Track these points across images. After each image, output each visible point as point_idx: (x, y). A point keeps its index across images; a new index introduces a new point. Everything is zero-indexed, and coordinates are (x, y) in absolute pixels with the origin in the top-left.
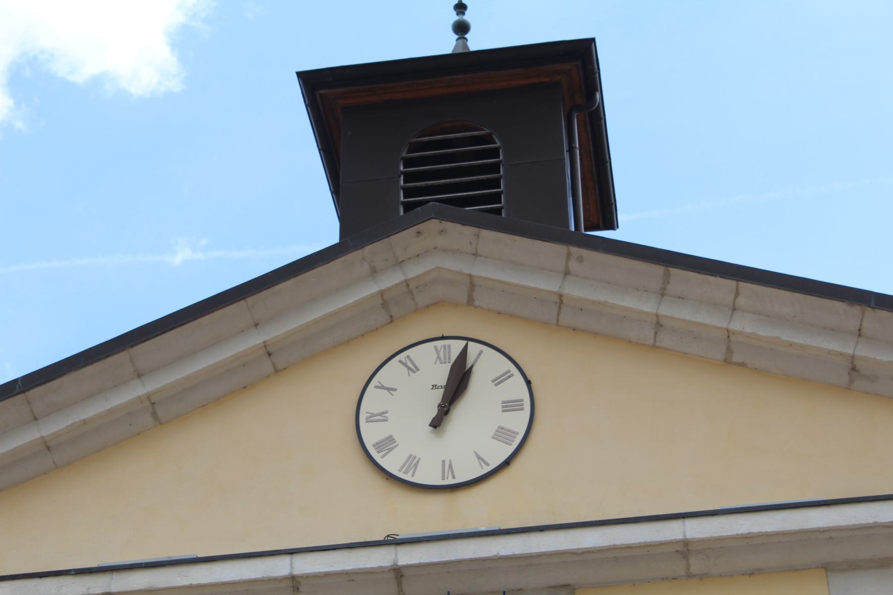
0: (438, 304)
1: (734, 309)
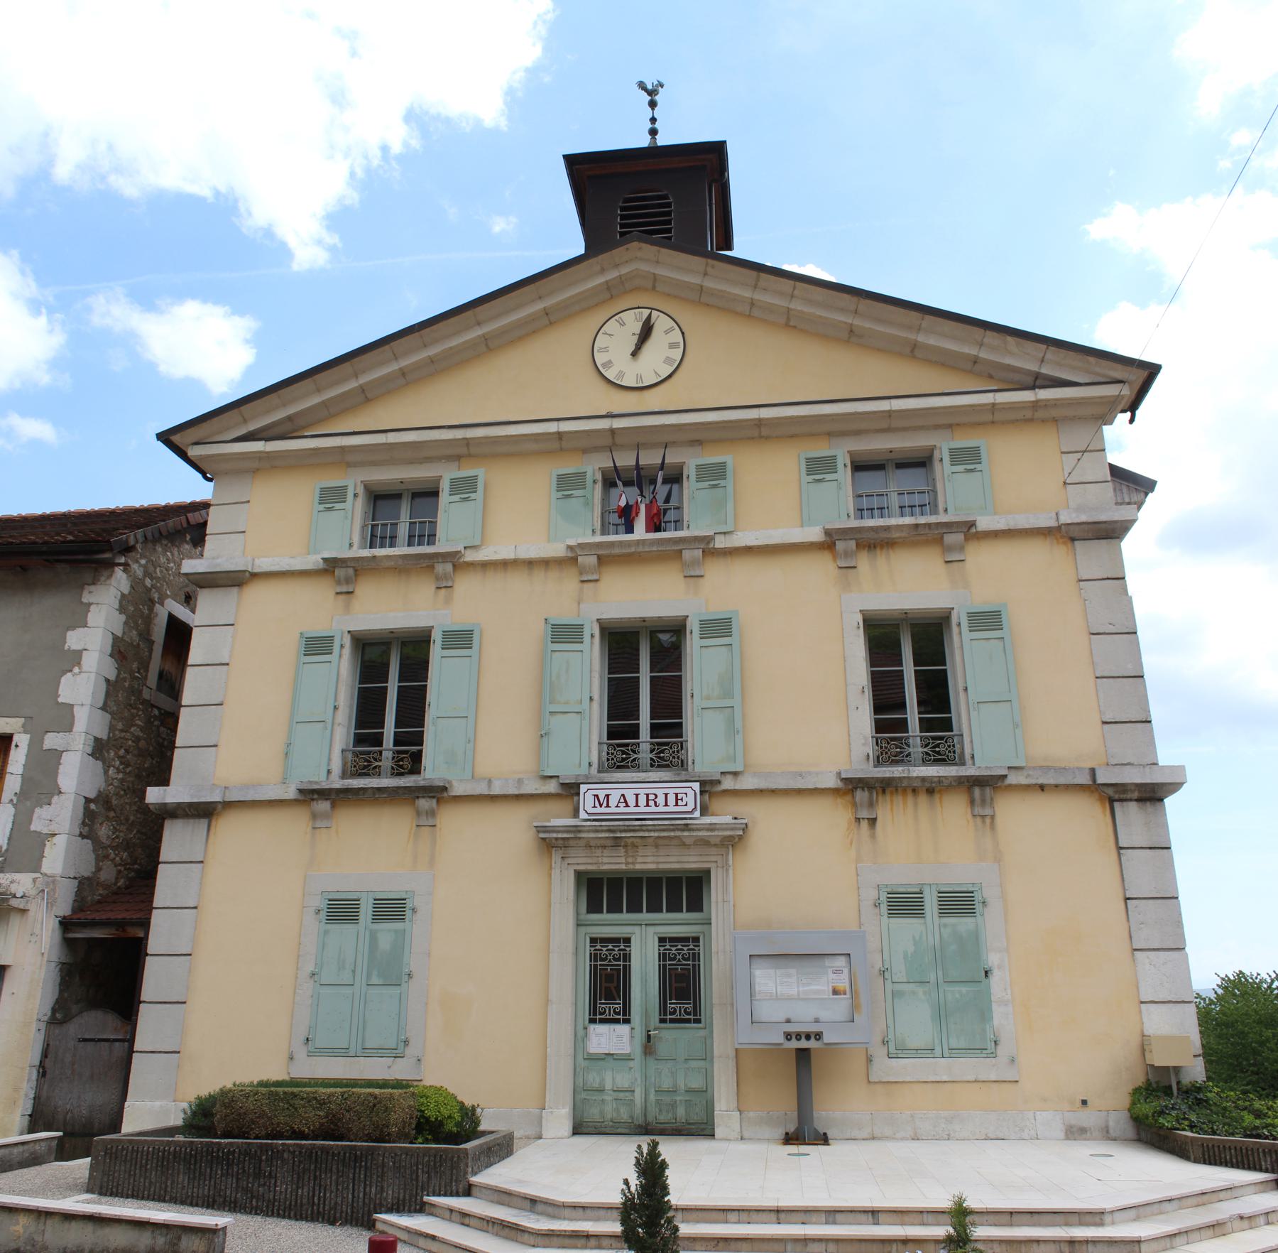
0: (637, 289)
1: (792, 296)
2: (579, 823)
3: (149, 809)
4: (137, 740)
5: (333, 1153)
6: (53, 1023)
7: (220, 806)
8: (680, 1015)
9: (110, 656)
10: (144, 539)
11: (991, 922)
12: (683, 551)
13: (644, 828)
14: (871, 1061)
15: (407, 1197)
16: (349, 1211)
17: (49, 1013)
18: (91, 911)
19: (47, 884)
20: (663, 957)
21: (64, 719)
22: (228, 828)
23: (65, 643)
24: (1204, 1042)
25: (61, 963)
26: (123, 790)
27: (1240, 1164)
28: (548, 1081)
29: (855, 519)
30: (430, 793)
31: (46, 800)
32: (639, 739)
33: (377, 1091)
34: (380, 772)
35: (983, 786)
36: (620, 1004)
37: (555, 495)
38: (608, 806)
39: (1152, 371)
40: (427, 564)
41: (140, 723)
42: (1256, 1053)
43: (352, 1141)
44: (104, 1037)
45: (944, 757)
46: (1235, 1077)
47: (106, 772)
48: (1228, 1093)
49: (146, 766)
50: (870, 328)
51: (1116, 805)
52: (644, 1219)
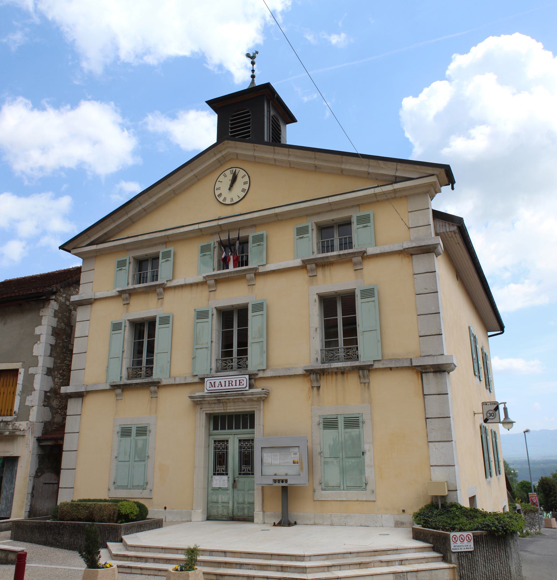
11: (366, 430)
17: (35, 474)
51: (424, 375)
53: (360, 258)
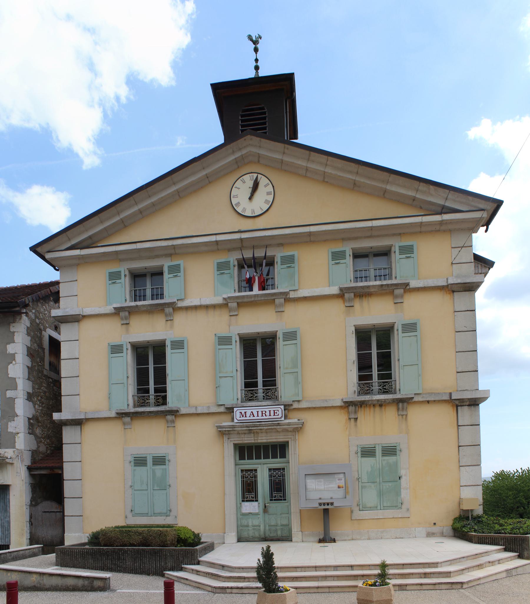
0: (250, 162)
1: (326, 165)
2: (234, 424)
3: (55, 421)
4: (45, 392)
5: (146, 551)
6: (32, 506)
7: (84, 420)
8: (278, 498)
9: (27, 355)
10: (32, 300)
11: (402, 458)
12: (276, 300)
13: (261, 425)
14: (352, 512)
15: (176, 566)
16: (154, 571)
17: (30, 502)
18: (38, 463)
19: (19, 453)
20: (270, 476)
21: (13, 384)
22: (89, 429)
23: (7, 350)
24: (485, 497)
25: (30, 483)
26: (43, 414)
27: (491, 543)
28: (226, 524)
29: (354, 282)
30: (172, 413)
31: (12, 419)
32: (258, 387)
33: (161, 529)
34: (150, 405)
35: (403, 402)
36: (254, 494)
37: (217, 273)
38: (246, 417)
39: (499, 204)
40: (160, 309)
41: (45, 385)
42: (504, 500)
43: (153, 547)
44: (52, 511)
45: (387, 390)
46: (495, 510)
47: (34, 407)
48: (491, 518)
49: (50, 403)
50: (364, 182)
51: (459, 408)
52: (265, 573)
53: (402, 291)
